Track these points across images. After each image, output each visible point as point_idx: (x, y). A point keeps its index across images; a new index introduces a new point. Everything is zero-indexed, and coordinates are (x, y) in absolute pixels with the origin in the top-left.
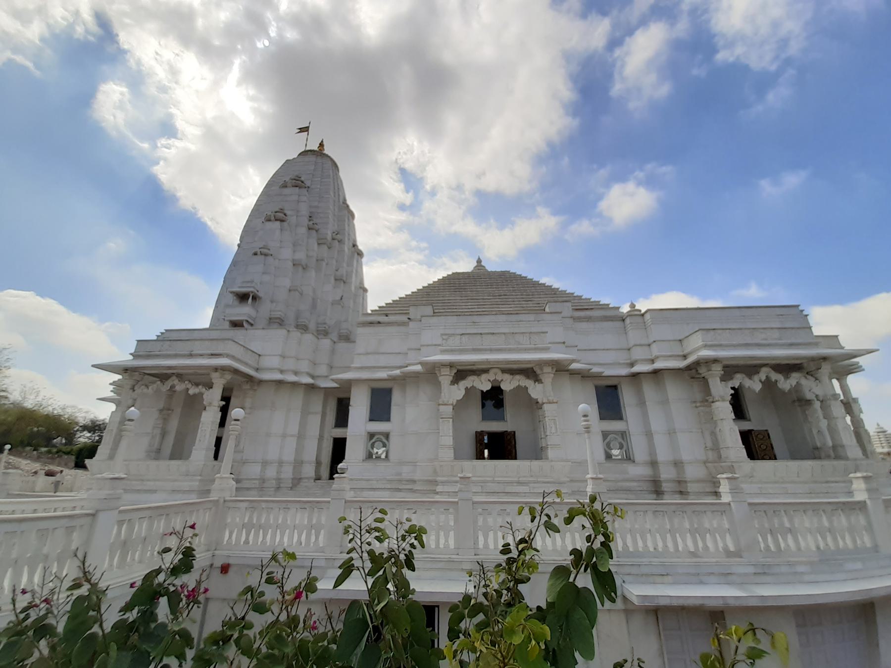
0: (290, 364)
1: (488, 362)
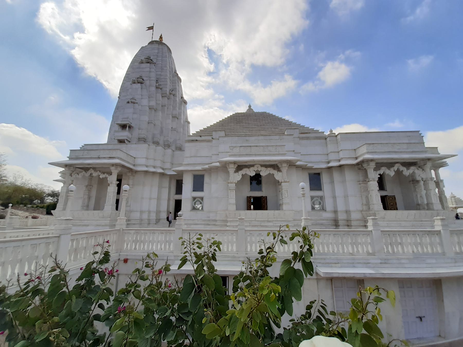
0: (151, 162)
1: (254, 161)
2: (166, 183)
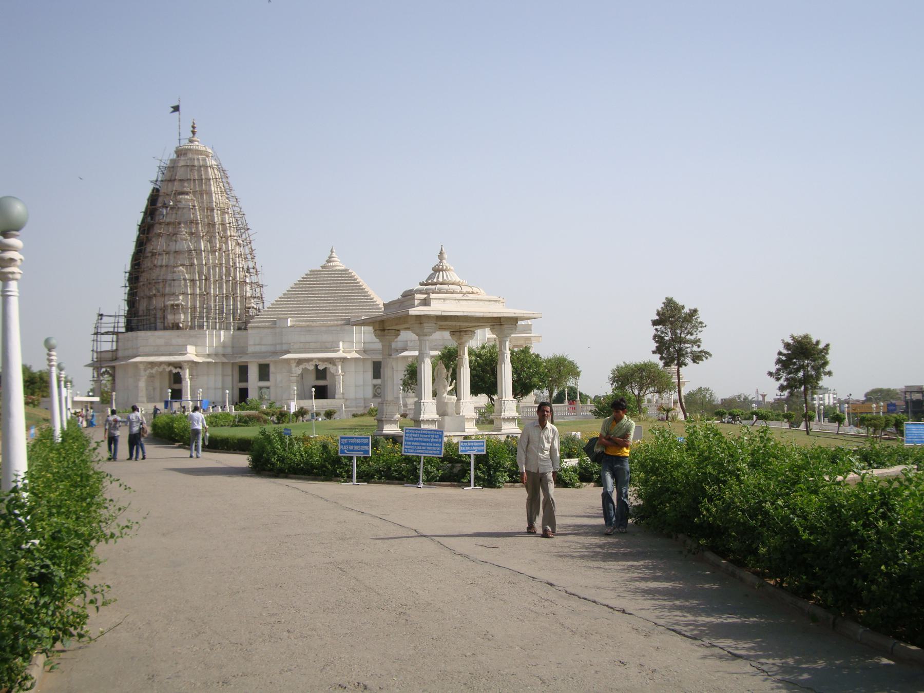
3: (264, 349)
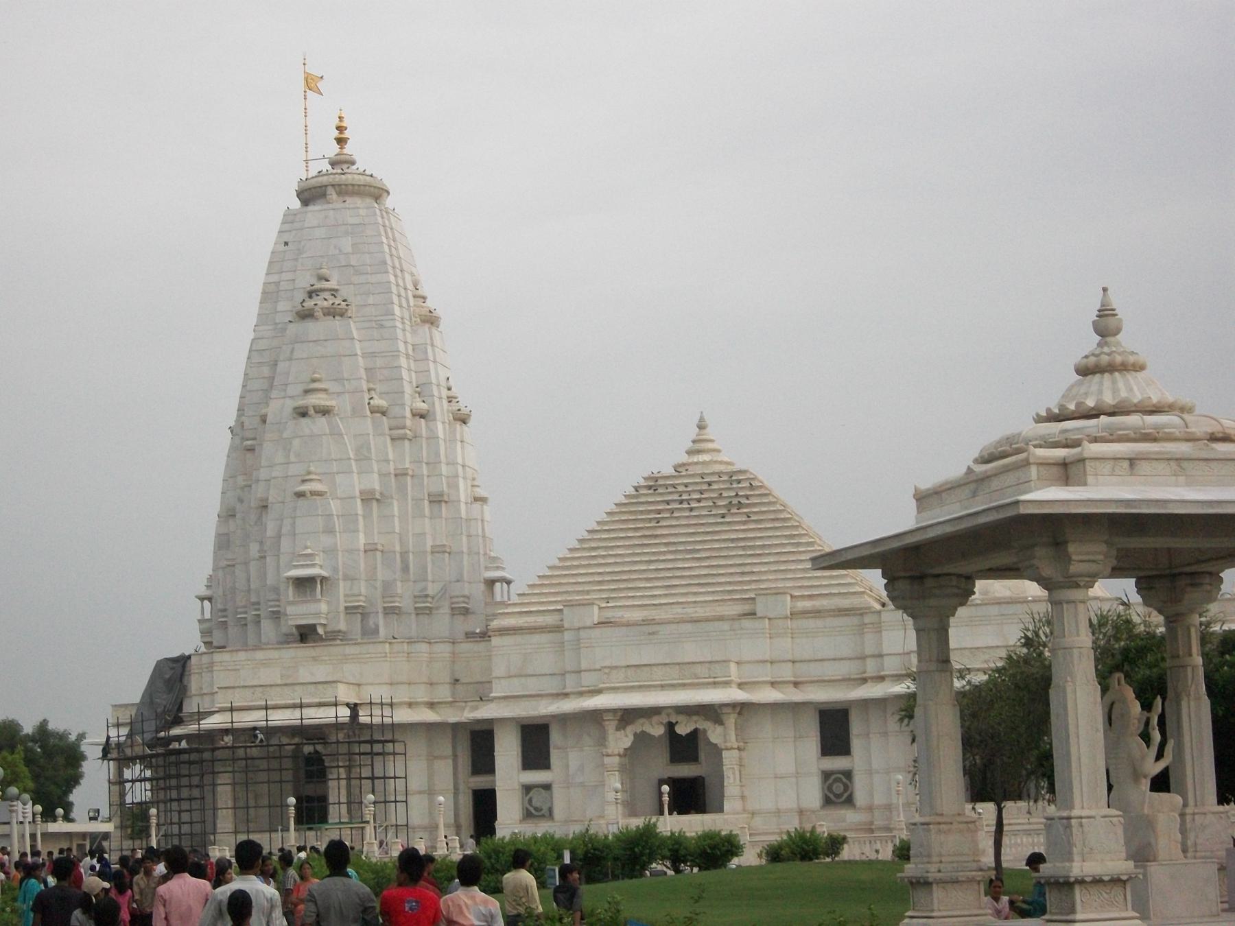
0: (402, 695)
2: (445, 746)
3: (533, 686)
